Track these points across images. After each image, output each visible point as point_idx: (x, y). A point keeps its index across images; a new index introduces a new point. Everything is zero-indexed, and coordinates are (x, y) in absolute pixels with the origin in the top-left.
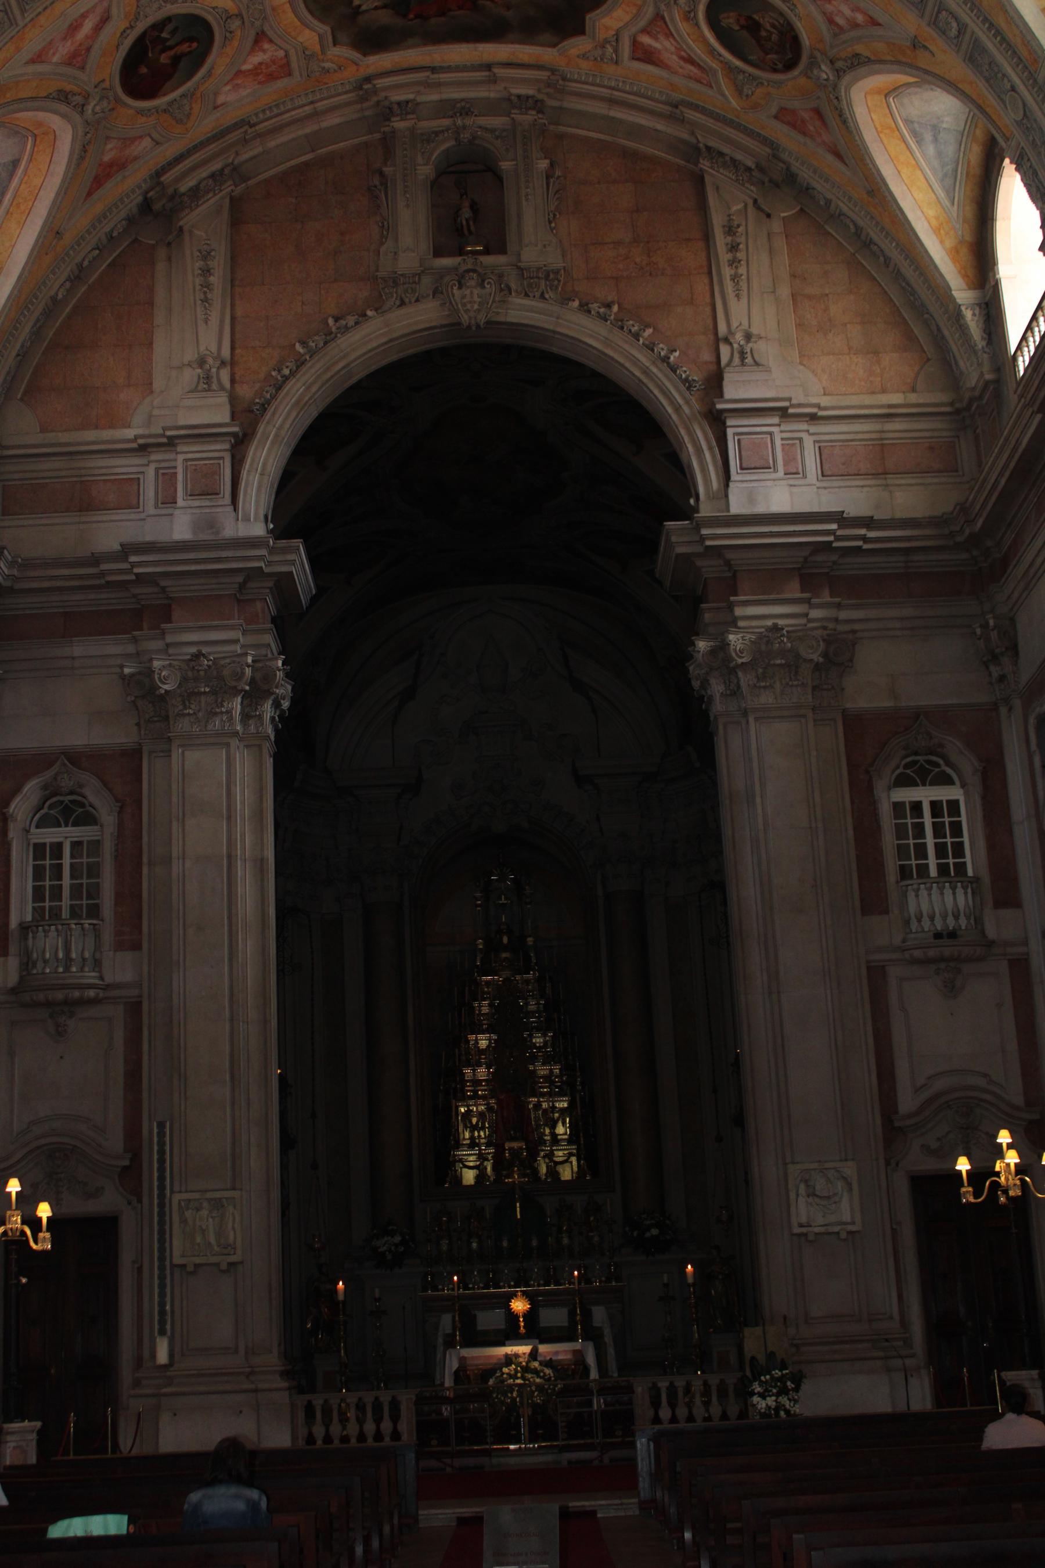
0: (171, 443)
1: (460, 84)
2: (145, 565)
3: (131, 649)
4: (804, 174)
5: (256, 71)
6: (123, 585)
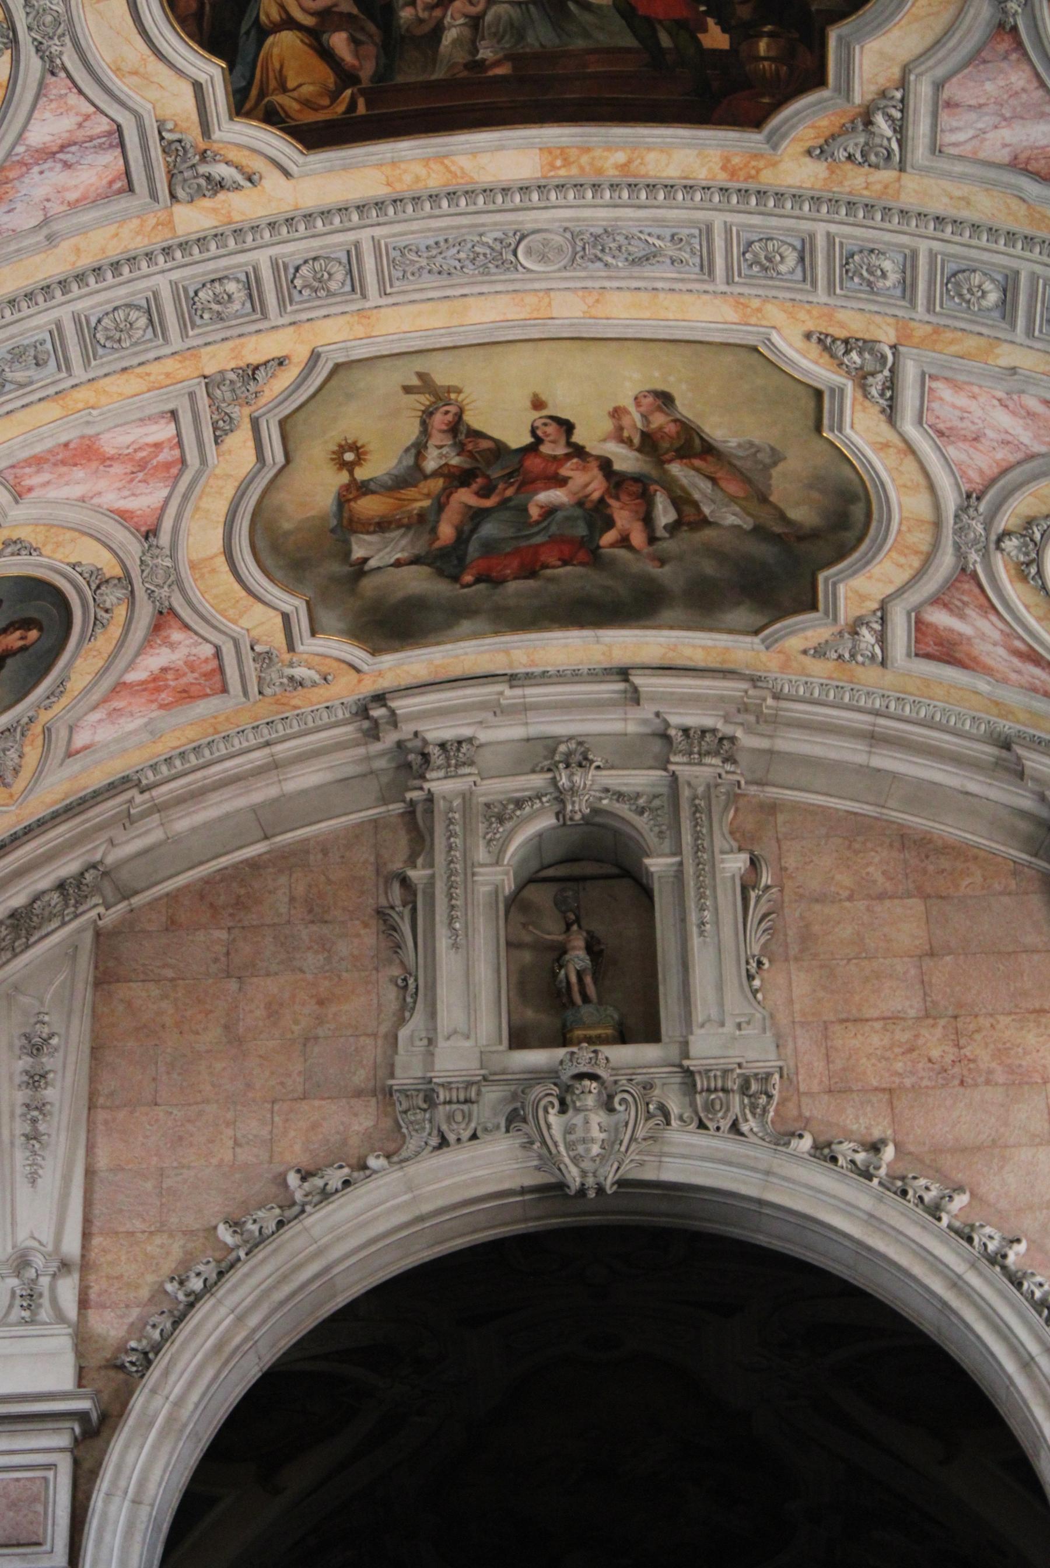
5: (155, 684)
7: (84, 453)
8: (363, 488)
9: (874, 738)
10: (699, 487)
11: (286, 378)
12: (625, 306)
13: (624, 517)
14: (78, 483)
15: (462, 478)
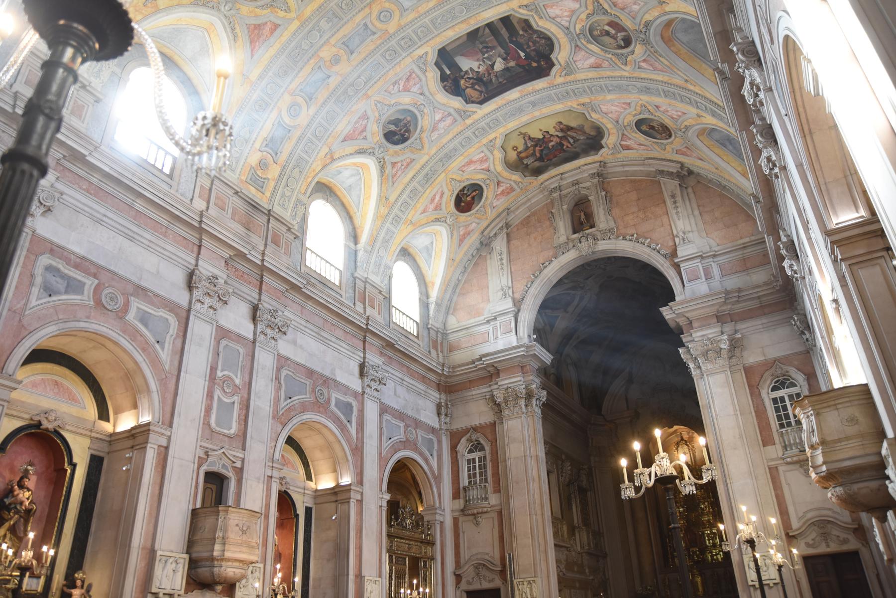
0: (495, 319)
1: (572, 176)
2: (487, 361)
3: (489, 389)
4: (695, 170)
5: (503, 193)
6: (484, 368)
7: (471, 162)
8: (520, 152)
9: (623, 166)
10: (574, 135)
11: (498, 140)
12: (546, 111)
13: (565, 143)
14: (472, 167)
15: (536, 146)
